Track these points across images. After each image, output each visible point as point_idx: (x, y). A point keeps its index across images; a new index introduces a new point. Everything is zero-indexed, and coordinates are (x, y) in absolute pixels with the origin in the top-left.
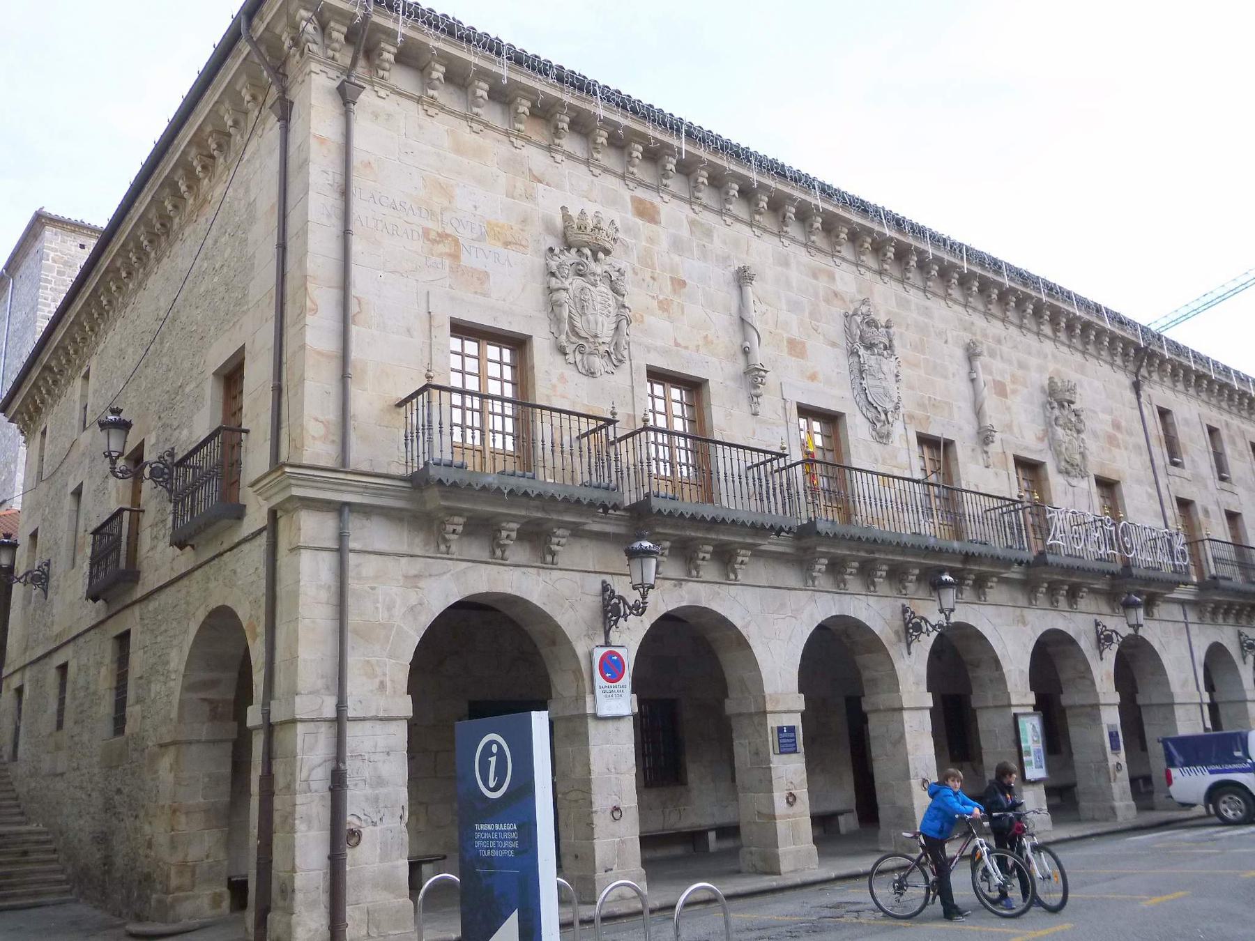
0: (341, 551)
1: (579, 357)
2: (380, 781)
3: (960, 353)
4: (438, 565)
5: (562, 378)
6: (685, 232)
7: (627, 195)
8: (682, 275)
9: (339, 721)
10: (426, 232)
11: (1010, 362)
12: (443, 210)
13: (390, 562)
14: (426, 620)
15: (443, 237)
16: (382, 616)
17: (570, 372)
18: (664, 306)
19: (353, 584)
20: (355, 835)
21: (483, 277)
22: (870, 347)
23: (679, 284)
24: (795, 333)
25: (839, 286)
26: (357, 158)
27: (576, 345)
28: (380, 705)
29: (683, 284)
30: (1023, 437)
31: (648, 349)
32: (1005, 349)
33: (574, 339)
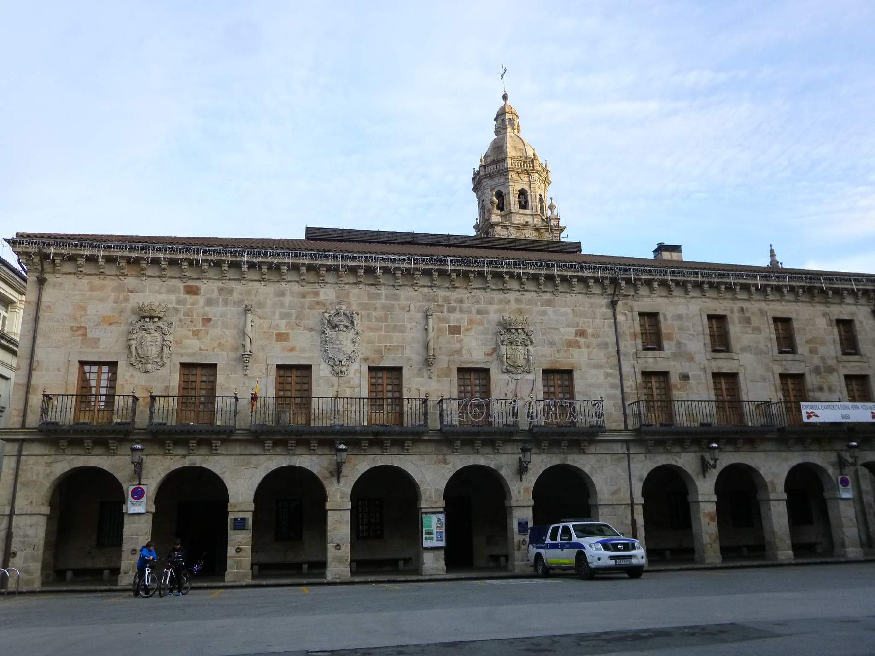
0: (19, 455)
1: (141, 366)
2: (26, 536)
4: (61, 458)
5: (132, 376)
6: (215, 295)
7: (181, 286)
8: (210, 316)
10: (72, 328)
11: (470, 312)
12: (82, 316)
13: (40, 459)
14: (53, 478)
15: (79, 328)
17: (137, 374)
18: (196, 334)
20: (14, 554)
21: (97, 341)
22: (334, 327)
23: (207, 320)
24: (283, 329)
25: (322, 297)
26: (43, 306)
27: (140, 361)
29: (210, 320)
31: (182, 355)
32: (465, 305)
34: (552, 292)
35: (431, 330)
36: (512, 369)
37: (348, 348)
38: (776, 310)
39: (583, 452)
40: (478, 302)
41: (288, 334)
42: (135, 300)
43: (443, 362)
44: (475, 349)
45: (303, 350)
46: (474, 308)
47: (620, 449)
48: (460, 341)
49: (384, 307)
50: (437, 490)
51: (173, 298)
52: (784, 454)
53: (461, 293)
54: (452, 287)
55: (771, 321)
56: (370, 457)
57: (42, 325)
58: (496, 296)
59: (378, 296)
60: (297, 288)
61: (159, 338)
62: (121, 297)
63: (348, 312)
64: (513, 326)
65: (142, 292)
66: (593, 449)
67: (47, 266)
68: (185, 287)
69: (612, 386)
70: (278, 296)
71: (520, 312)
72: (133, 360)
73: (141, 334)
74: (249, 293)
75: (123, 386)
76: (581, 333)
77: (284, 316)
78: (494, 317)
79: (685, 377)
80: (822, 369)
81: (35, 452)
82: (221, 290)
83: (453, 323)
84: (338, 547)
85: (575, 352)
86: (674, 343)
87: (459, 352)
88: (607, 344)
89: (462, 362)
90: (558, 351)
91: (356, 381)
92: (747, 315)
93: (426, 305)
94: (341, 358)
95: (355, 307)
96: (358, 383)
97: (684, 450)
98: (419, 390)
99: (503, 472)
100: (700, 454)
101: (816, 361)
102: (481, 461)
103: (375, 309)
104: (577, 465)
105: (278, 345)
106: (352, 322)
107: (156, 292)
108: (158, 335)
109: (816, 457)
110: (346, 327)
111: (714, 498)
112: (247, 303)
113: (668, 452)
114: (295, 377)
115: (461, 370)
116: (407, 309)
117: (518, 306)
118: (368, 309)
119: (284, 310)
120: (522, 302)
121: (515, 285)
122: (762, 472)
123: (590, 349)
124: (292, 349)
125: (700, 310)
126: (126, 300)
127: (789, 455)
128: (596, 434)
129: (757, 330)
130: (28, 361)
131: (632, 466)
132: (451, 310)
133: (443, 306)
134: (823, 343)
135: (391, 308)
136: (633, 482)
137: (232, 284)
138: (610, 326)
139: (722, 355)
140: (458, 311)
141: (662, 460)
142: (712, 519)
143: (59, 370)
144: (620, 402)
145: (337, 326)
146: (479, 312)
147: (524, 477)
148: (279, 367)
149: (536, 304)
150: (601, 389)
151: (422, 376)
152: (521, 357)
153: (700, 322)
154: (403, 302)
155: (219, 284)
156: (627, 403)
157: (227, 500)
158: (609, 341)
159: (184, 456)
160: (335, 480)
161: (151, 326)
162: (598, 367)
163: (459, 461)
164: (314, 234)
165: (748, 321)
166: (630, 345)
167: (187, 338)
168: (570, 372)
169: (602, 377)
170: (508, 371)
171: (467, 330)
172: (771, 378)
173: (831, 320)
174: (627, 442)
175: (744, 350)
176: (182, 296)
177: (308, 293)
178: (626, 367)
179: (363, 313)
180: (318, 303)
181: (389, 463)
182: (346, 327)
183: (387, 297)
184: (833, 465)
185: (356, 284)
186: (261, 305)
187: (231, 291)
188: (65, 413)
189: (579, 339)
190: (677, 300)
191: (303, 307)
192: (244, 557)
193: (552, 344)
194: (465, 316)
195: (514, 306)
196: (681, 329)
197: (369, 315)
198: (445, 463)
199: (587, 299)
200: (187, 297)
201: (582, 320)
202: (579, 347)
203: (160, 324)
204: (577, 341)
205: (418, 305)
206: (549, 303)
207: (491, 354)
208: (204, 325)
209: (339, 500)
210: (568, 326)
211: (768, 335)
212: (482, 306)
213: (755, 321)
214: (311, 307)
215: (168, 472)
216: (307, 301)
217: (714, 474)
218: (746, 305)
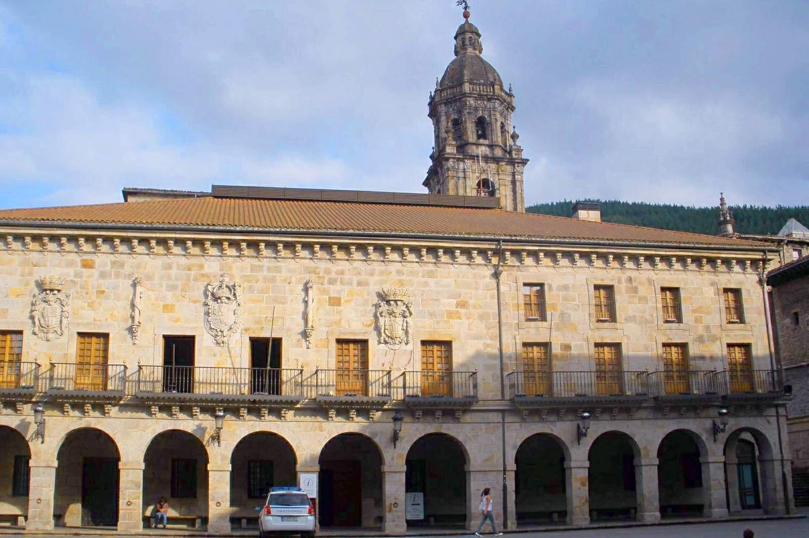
3: (301, 287)
5: (35, 344)
6: (108, 268)
11: (350, 283)
17: (39, 342)
18: (91, 305)
22: (216, 299)
24: (169, 301)
25: (206, 270)
29: (103, 292)
31: (78, 325)
32: (347, 277)
33: (41, 328)
34: (435, 263)
35: (310, 302)
36: (390, 340)
37: (230, 319)
39: (457, 420)
40: (359, 274)
46: (355, 279)
47: (497, 417)
48: (339, 312)
49: (266, 280)
51: (71, 271)
55: (658, 290)
58: (378, 267)
60: (183, 261)
61: (59, 310)
62: (27, 271)
63: (230, 284)
64: (392, 298)
65: (44, 266)
66: (468, 417)
68: (82, 260)
70: (166, 269)
72: (36, 330)
73: (44, 305)
74: (138, 266)
75: (28, 352)
76: (462, 305)
77: (173, 288)
78: (375, 288)
80: (706, 338)
82: (114, 263)
83: (333, 295)
84: (218, 504)
86: (557, 314)
87: (338, 323)
89: (341, 333)
90: (438, 323)
93: (307, 277)
94: (222, 329)
95: (238, 281)
97: (560, 419)
98: (297, 360)
100: (576, 423)
101: (701, 330)
103: (257, 281)
105: (166, 316)
106: (235, 294)
107: (57, 264)
108: (57, 306)
109: (691, 424)
110: (228, 298)
111: (587, 464)
112: (136, 276)
113: (542, 420)
115: (339, 341)
116: (288, 281)
117: (398, 278)
118: (249, 281)
119: (171, 283)
120: (403, 274)
121: (395, 256)
122: (636, 439)
123: (471, 320)
124: (177, 320)
126: (30, 274)
127: (667, 422)
128: (470, 404)
129: (643, 299)
132: (332, 282)
133: (324, 277)
134: (708, 313)
138: (492, 298)
139: (606, 325)
140: (338, 283)
142: (583, 484)
145: (219, 298)
146: (359, 284)
147: (398, 444)
149: (418, 275)
151: (301, 347)
152: (400, 327)
153: (586, 293)
154: (284, 274)
156: (505, 374)
157: (118, 459)
161: (51, 297)
165: (635, 290)
166: (513, 314)
167: (83, 308)
170: (386, 343)
172: (655, 347)
174: (503, 411)
176: (79, 268)
177: (193, 265)
179: (246, 285)
180: (203, 275)
182: (228, 298)
183: (269, 269)
184: (707, 432)
185: (238, 257)
186: (149, 278)
187: (122, 265)
189: (460, 310)
191: (188, 279)
192: (135, 510)
193: (432, 315)
194: (346, 288)
195: (394, 277)
200: (84, 270)
203: (59, 295)
205: (299, 276)
206: (431, 274)
208: (97, 297)
209: (220, 462)
210: (450, 297)
211: (655, 302)
212: (363, 277)
213: (643, 291)
214: (196, 280)
215: (67, 432)
217: (588, 441)
218: (634, 274)
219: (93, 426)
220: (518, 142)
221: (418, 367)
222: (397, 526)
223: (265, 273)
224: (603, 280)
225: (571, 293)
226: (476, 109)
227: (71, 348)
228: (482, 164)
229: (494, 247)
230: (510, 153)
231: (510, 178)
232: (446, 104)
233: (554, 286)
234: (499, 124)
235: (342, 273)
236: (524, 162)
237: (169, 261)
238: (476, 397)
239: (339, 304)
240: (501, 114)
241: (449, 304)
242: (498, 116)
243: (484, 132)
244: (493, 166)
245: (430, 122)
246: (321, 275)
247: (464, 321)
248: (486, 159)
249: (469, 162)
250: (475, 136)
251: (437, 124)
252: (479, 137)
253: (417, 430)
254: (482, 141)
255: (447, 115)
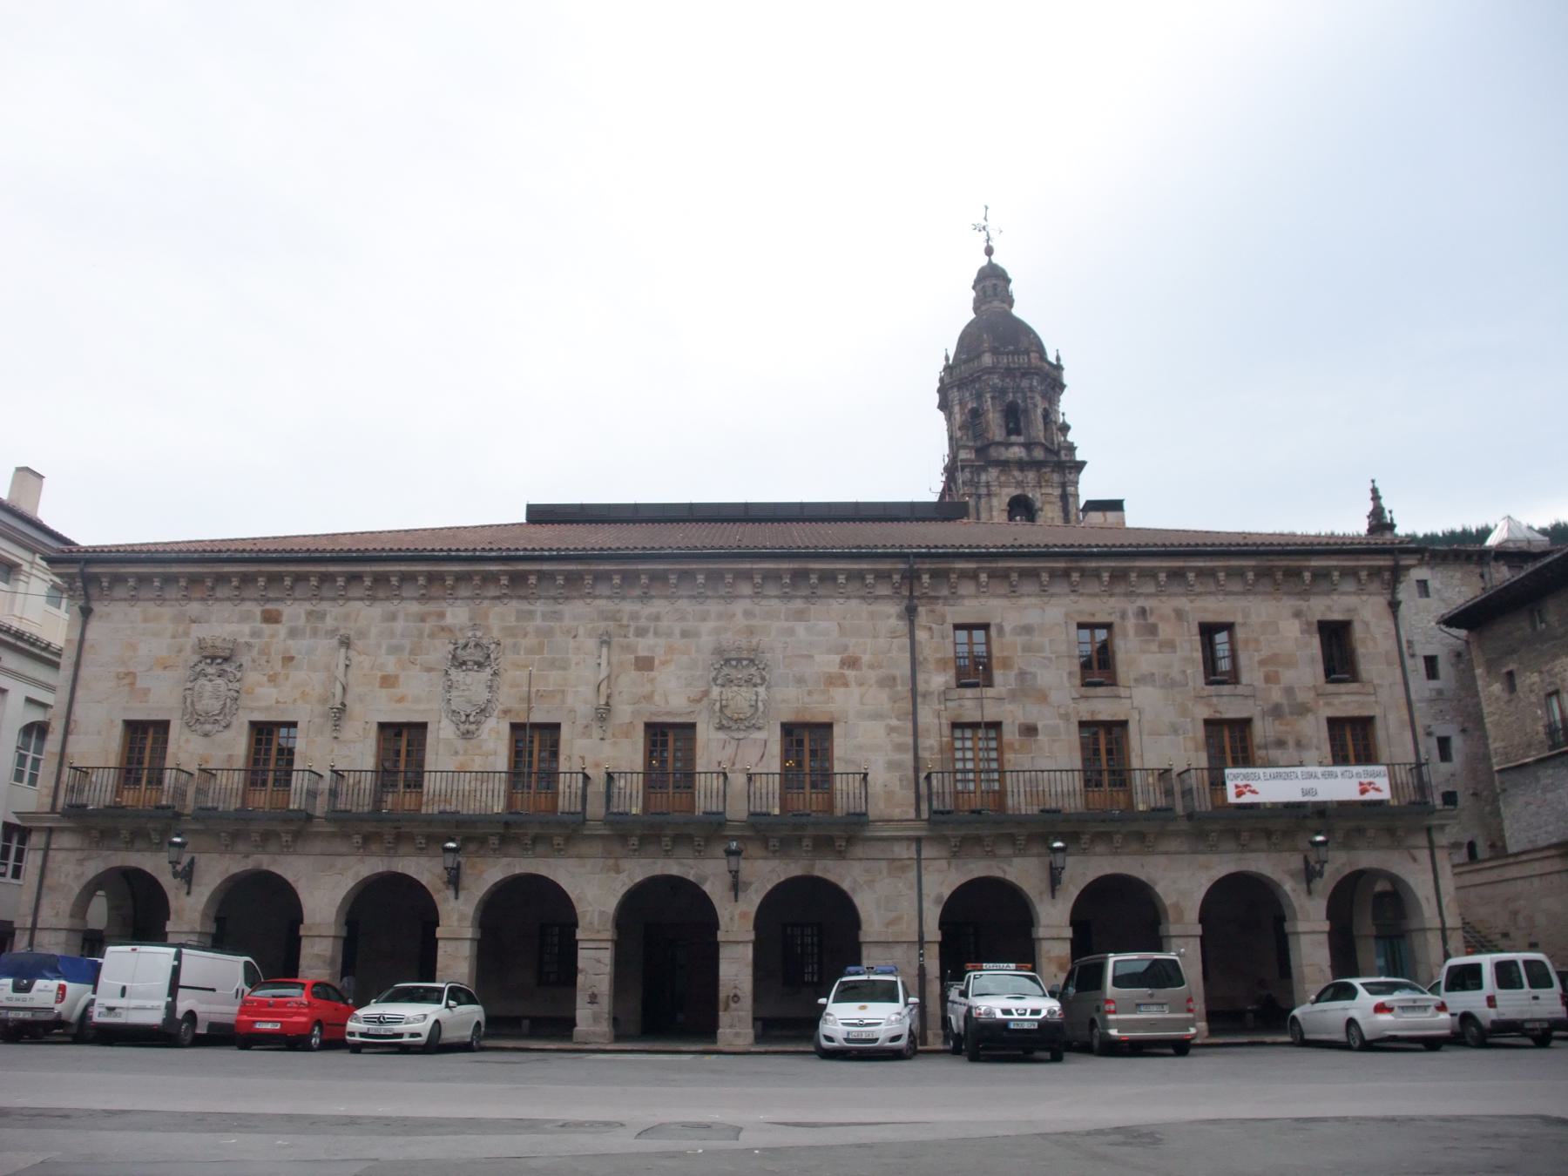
5: (187, 741)
6: (302, 622)
8: (293, 653)
9: (34, 928)
11: (670, 634)
14: (84, 881)
15: (127, 674)
16: (63, 880)
17: (194, 738)
18: (272, 679)
19: (50, 865)
21: (146, 691)
25: (449, 620)
26: (86, 645)
27: (196, 719)
28: (54, 922)
29: (291, 659)
30: (667, 702)
31: (252, 710)
32: (664, 624)
34: (806, 597)
38: (1205, 610)
39: (841, 855)
40: (683, 619)
41: (397, 677)
42: (198, 631)
43: (624, 712)
44: (672, 695)
45: (417, 700)
47: (904, 851)
48: (652, 681)
49: (539, 632)
50: (602, 913)
51: (246, 628)
52: (1202, 858)
53: (658, 606)
54: (645, 597)
55: (1195, 630)
56: (505, 860)
57: (84, 672)
58: (714, 607)
59: (530, 615)
60: (415, 607)
62: (181, 630)
64: (733, 655)
66: (858, 850)
67: (93, 591)
69: (899, 748)
71: (751, 631)
74: (346, 617)
76: (851, 663)
77: (394, 650)
78: (707, 641)
79: (1030, 730)
80: (1287, 709)
81: (67, 845)
82: (310, 614)
83: (641, 653)
85: (838, 693)
86: (1013, 674)
87: (649, 698)
88: (894, 679)
89: (652, 714)
90: (810, 693)
91: (490, 746)
92: (1152, 620)
93: (602, 625)
95: (496, 634)
96: (494, 747)
97: (1021, 852)
98: (583, 758)
99: (707, 888)
100: (1047, 860)
101: (1276, 695)
102: (673, 868)
103: (525, 635)
104: (831, 877)
106: (488, 657)
107: (226, 622)
109: (1262, 863)
111: (1068, 932)
112: (342, 632)
114: (402, 741)
119: (394, 642)
122: (1159, 889)
124: (401, 700)
125: (1067, 615)
126: (186, 634)
127: (1214, 858)
129: (1169, 645)
130: (63, 721)
131: (924, 878)
132: (641, 632)
134: (1291, 664)
135: (549, 633)
136: (925, 905)
137: (325, 606)
139: (1100, 691)
141: (978, 868)
143: (99, 733)
144: (911, 773)
146: (684, 634)
147: (741, 895)
148: (383, 726)
150: (874, 757)
151: (590, 737)
155: (308, 606)
157: (301, 921)
158: (898, 673)
159: (247, 856)
160: (451, 893)
161: (210, 670)
162: (877, 716)
163: (638, 870)
164: (539, 515)
165: (1152, 630)
166: (937, 680)
167: (260, 685)
168: (828, 727)
169: (882, 732)
171: (664, 663)
172: (1189, 727)
173: (1309, 624)
174: (918, 840)
175: (1143, 680)
177: (429, 614)
178: (926, 716)
180: (443, 629)
181: (532, 870)
183: (544, 616)
184: (1293, 875)
185: (498, 598)
186: (362, 634)
187: (322, 616)
188: (101, 792)
190: (1026, 601)
191: (421, 635)
193: (800, 681)
194: (662, 641)
195: (741, 621)
196: (1027, 649)
197: (515, 645)
198: (618, 871)
199: (865, 606)
200: (264, 626)
201: (854, 641)
202: (846, 685)
203: (226, 667)
204: (843, 676)
206: (800, 616)
207: (699, 701)
210: (829, 651)
213: (1165, 631)
214: (432, 636)
216: (428, 626)
218: (1148, 603)
219: (265, 867)
220: (1071, 437)
221: (776, 766)
222: (737, 1035)
223: (539, 622)
224: (1093, 615)
225: (1037, 639)
226: (1003, 392)
227: (237, 744)
228: (1016, 473)
229: (902, 566)
230: (1057, 453)
231: (1057, 492)
232: (960, 387)
233: (1007, 628)
234: (1039, 411)
235: (657, 618)
236: (1082, 464)
237: (392, 608)
238: (865, 814)
239: (651, 668)
240: (1044, 397)
241: (829, 662)
242: (1038, 399)
243: (1017, 423)
244: (1031, 476)
245: (941, 415)
246: (625, 622)
247: (855, 691)
248: (1022, 465)
249: (993, 473)
250: (1004, 433)
251: (949, 418)
252: (1009, 433)
253: (772, 871)
254: (1014, 438)
255: (962, 403)
